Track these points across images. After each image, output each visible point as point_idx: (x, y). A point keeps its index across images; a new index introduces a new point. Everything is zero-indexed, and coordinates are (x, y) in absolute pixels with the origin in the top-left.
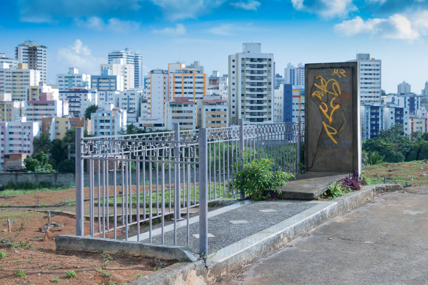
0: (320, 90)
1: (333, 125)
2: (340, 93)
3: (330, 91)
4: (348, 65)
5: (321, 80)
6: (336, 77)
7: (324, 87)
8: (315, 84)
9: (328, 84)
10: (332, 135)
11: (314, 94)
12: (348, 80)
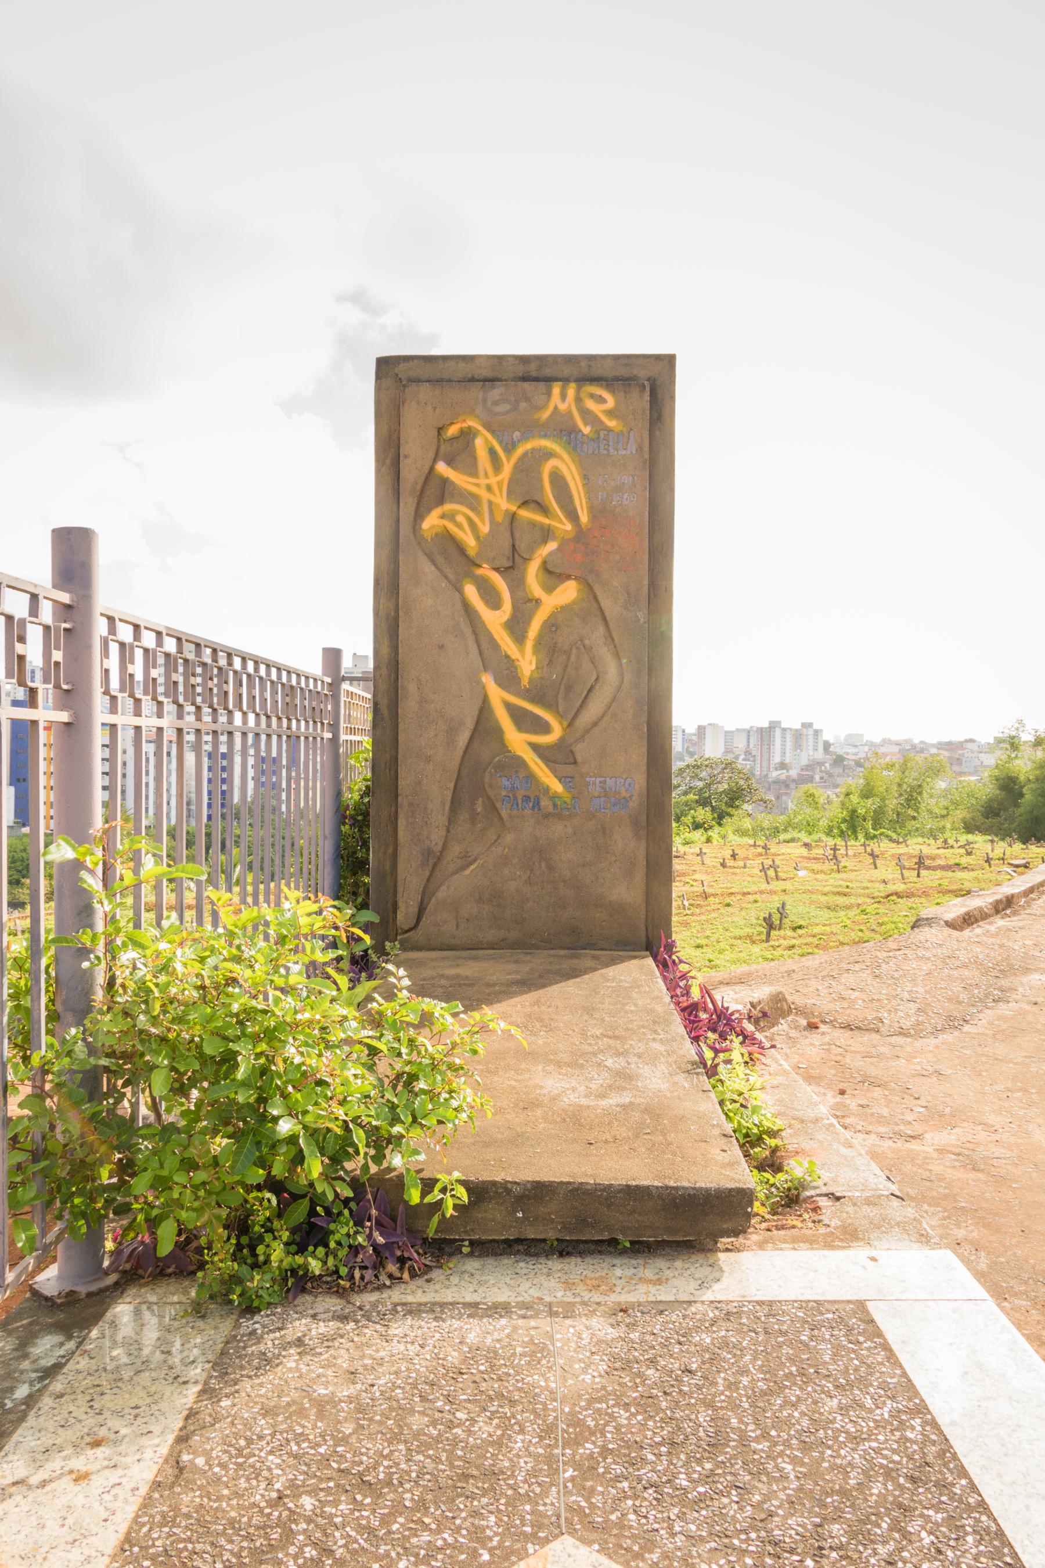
0: (472, 501)
1: (538, 694)
3: (525, 504)
4: (623, 372)
5: (479, 442)
7: (493, 480)
8: (442, 468)
9: (516, 467)
10: (535, 747)
11: (432, 522)
12: (632, 447)
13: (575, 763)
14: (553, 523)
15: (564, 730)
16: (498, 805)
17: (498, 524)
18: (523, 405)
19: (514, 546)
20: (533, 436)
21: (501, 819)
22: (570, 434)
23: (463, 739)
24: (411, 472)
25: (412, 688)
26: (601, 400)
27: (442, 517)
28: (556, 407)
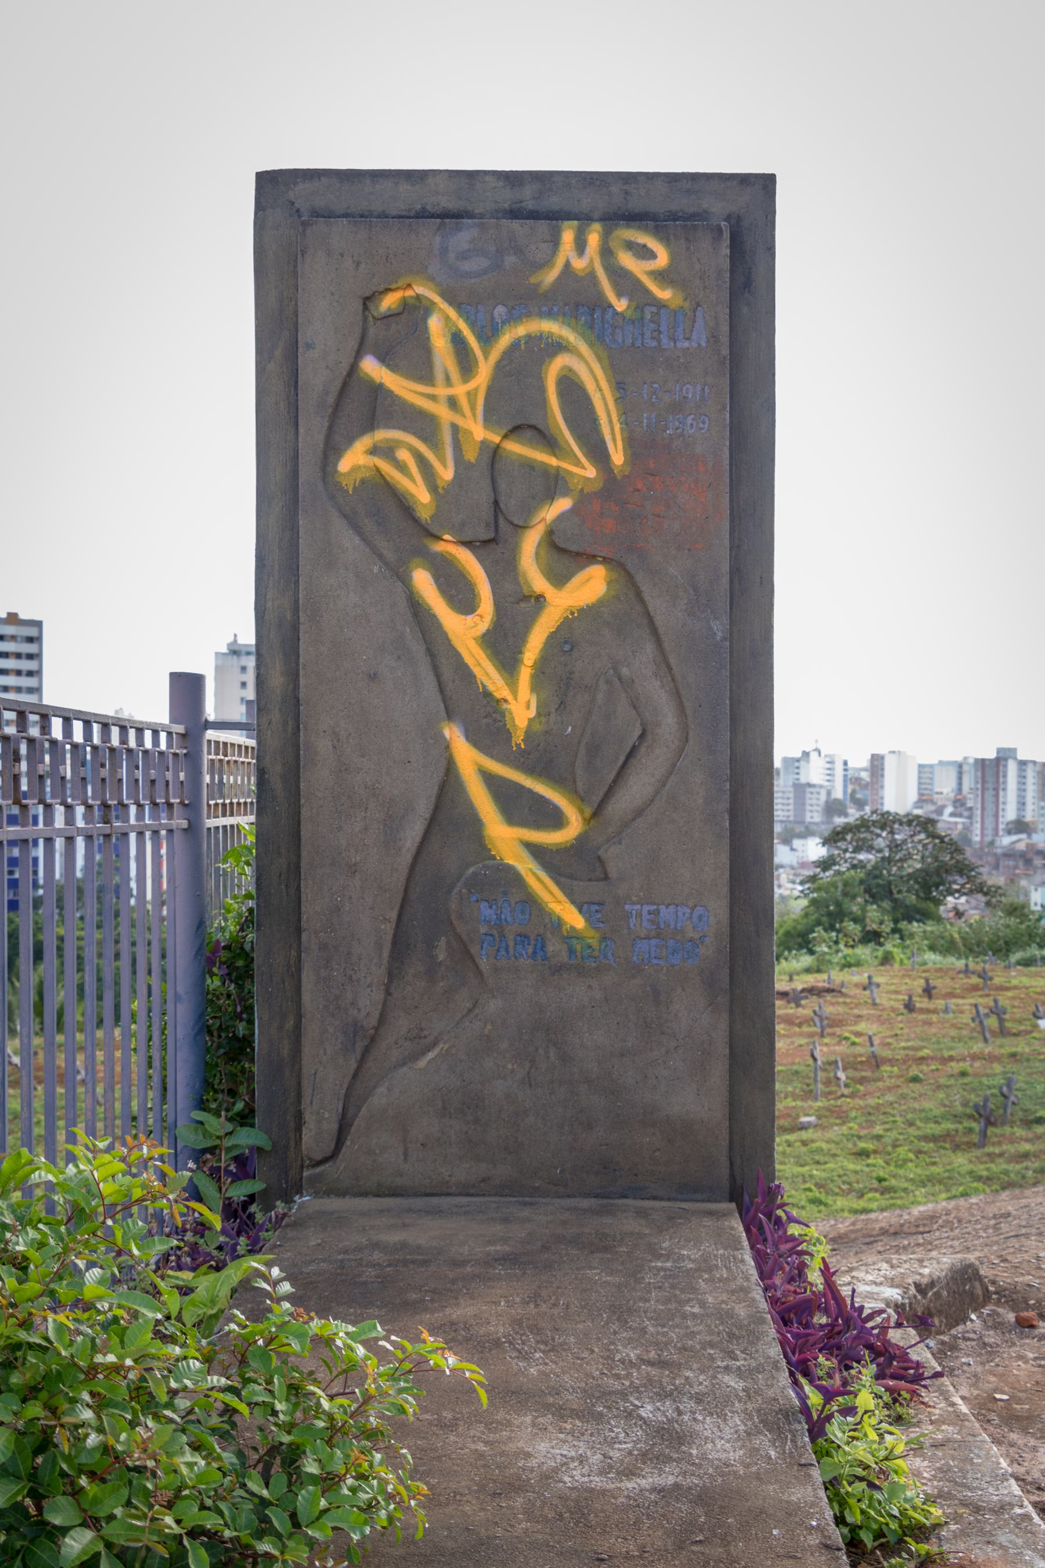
0: (422, 425)
1: (539, 757)
2: (618, 457)
3: (515, 431)
5: (434, 324)
6: (579, 301)
7: (460, 390)
8: (371, 367)
9: (499, 367)
10: (537, 851)
13: (606, 878)
14: (564, 465)
15: (587, 821)
16: (474, 950)
17: (469, 466)
18: (510, 260)
19: (496, 503)
20: (529, 315)
21: (479, 973)
22: (592, 310)
23: (412, 834)
24: (318, 377)
25: (323, 746)
26: (644, 253)
27: (374, 451)
28: (568, 264)
